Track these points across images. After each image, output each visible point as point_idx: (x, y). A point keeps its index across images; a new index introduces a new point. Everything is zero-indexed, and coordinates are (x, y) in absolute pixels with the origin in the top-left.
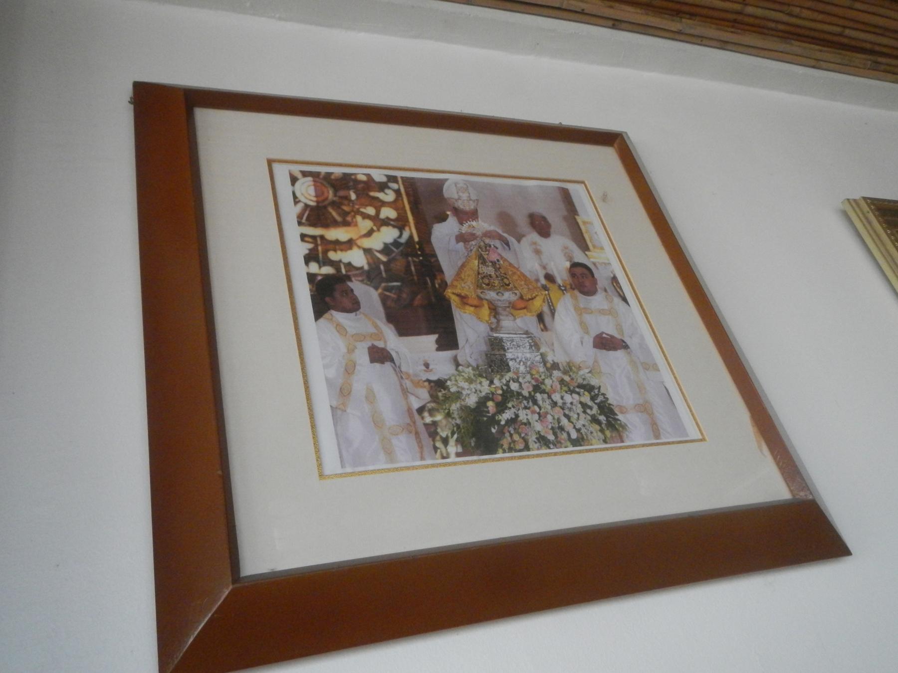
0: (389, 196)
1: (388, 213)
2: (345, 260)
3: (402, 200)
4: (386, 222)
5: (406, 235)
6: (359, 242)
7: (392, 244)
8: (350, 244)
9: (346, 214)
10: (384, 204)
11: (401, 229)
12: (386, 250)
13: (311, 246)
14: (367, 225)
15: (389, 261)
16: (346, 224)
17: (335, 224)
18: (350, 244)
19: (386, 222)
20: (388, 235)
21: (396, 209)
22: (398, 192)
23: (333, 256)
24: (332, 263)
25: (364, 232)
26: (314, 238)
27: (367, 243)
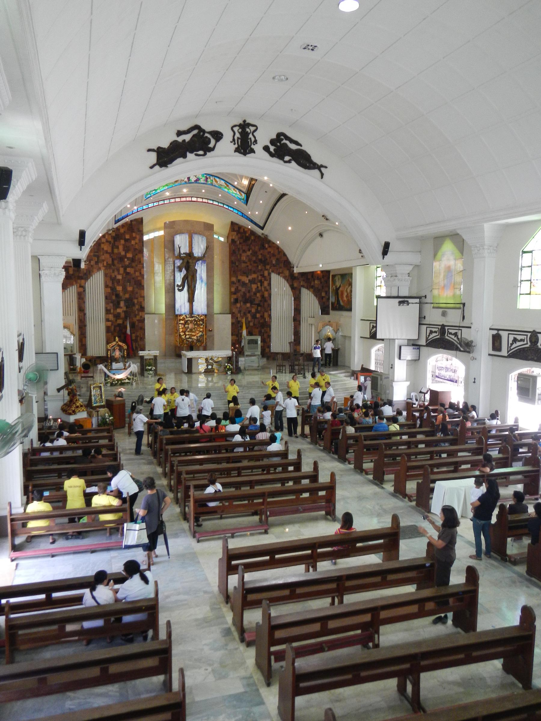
0: (202, 327)
1: (201, 330)
4: (201, 331)
12: (200, 336)
14: (198, 332)
17: (193, 332)
18: (195, 335)
19: (201, 331)
20: (200, 333)
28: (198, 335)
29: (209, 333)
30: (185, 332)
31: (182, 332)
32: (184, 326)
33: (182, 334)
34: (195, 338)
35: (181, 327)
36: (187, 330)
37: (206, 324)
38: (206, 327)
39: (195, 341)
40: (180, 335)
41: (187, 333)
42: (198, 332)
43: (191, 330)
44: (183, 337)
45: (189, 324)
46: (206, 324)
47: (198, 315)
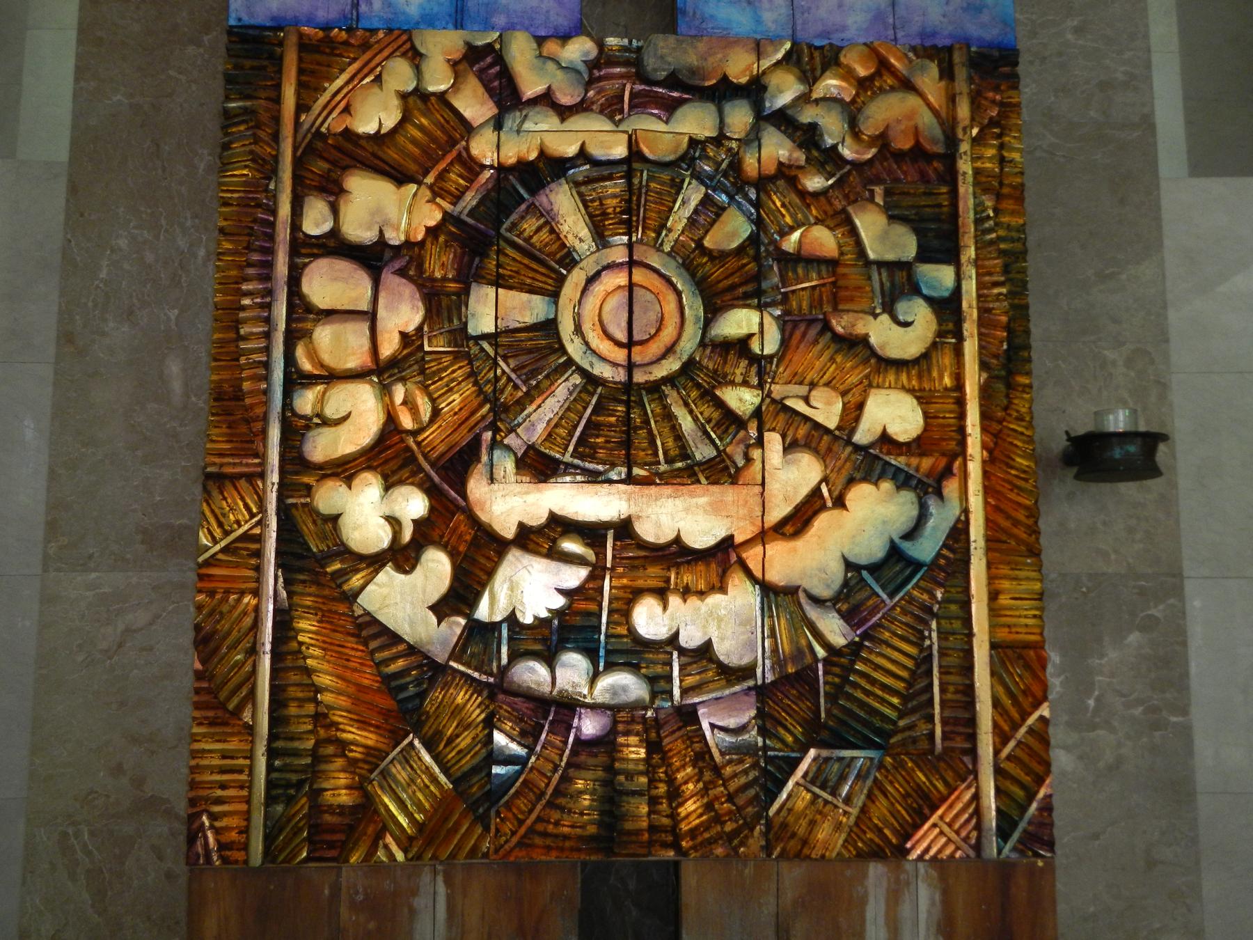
0: (902, 334)
1: (894, 414)
2: (691, 638)
3: (958, 352)
4: (875, 461)
5: (941, 519)
6: (752, 557)
7: (874, 569)
8: (723, 558)
9: (730, 420)
10: (884, 366)
11: (926, 488)
13: (574, 577)
14: (792, 476)
15: (854, 649)
16: (721, 471)
19: (875, 461)
20: (872, 516)
21: (923, 398)
22: (947, 308)
23: (649, 620)
24: (635, 653)
25: (778, 512)
26: (592, 533)
27: (784, 562)
28: (811, 561)
29: (1086, 526)
30: (447, 477)
31: (389, 457)
32: (443, 305)
33: (369, 512)
34: (722, 620)
35: (338, 345)
36: (501, 413)
37: (1010, 264)
38: (1009, 365)
39: (723, 720)
40: (318, 559)
41: (507, 501)
42: (792, 476)
43: (618, 430)
44: (404, 601)
45: (549, 268)
46: (1010, 264)
47: (810, 60)
